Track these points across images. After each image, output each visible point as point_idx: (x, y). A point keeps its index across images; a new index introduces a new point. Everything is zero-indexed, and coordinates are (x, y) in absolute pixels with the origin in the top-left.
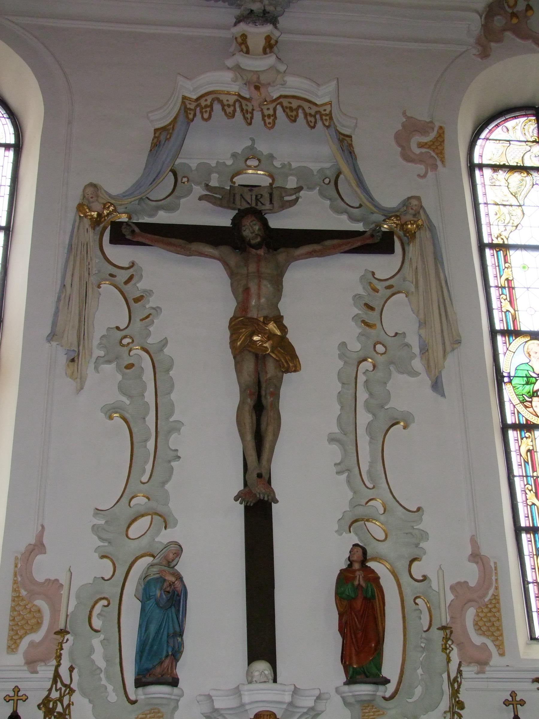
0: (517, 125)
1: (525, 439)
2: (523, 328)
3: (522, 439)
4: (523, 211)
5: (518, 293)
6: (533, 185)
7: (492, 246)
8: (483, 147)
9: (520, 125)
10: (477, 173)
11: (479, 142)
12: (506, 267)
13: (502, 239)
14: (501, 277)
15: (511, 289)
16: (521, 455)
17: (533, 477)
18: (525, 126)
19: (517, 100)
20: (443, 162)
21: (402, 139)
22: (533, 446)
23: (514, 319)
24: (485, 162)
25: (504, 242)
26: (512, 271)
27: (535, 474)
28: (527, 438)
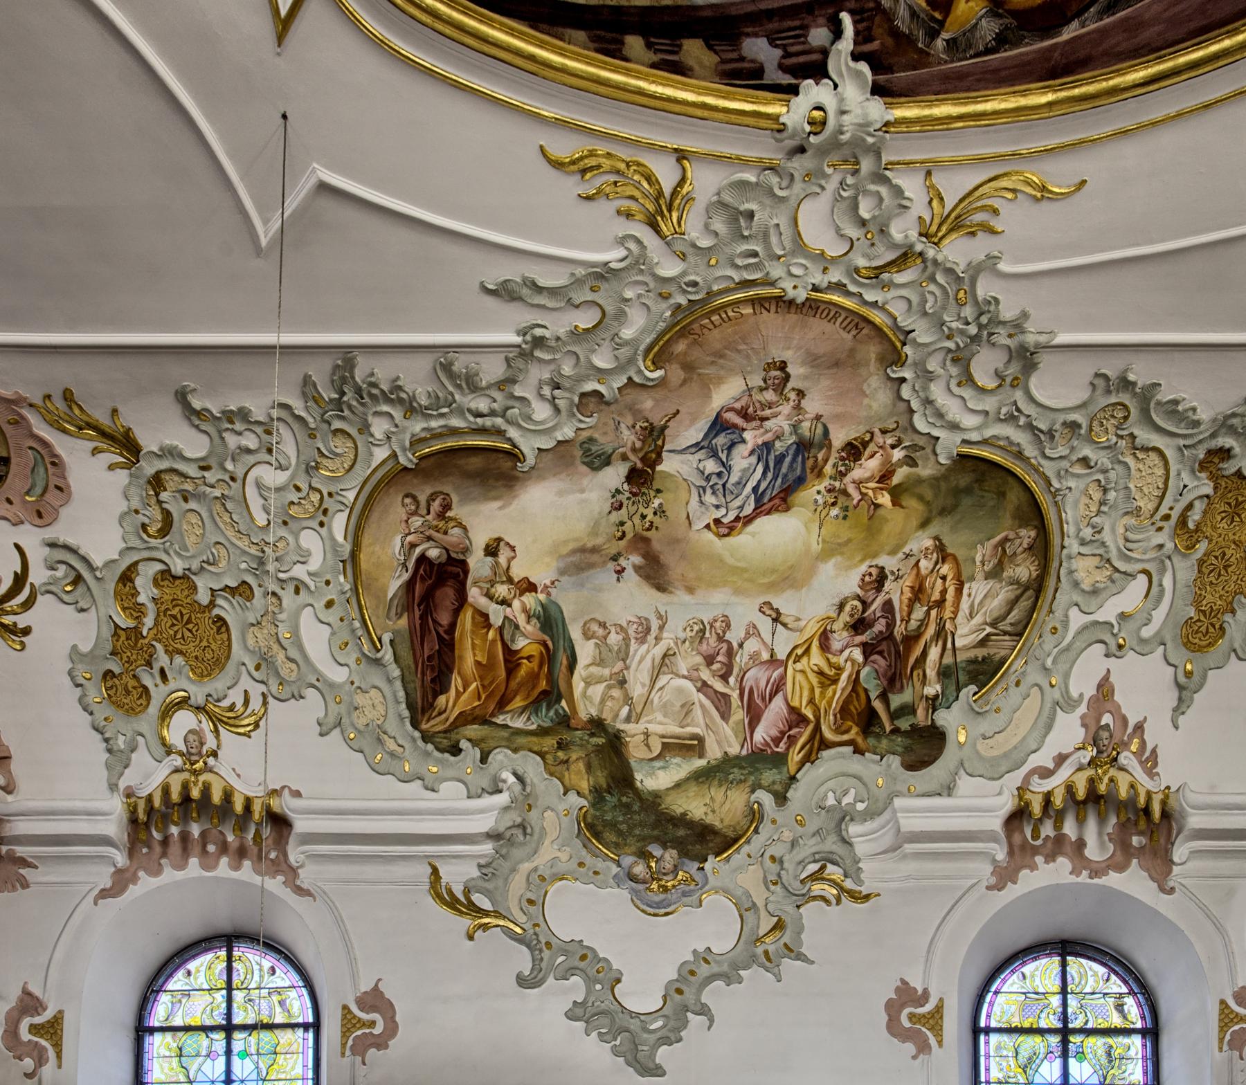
8: (991, 1004)
10: (982, 1038)
11: (989, 997)
24: (993, 1024)
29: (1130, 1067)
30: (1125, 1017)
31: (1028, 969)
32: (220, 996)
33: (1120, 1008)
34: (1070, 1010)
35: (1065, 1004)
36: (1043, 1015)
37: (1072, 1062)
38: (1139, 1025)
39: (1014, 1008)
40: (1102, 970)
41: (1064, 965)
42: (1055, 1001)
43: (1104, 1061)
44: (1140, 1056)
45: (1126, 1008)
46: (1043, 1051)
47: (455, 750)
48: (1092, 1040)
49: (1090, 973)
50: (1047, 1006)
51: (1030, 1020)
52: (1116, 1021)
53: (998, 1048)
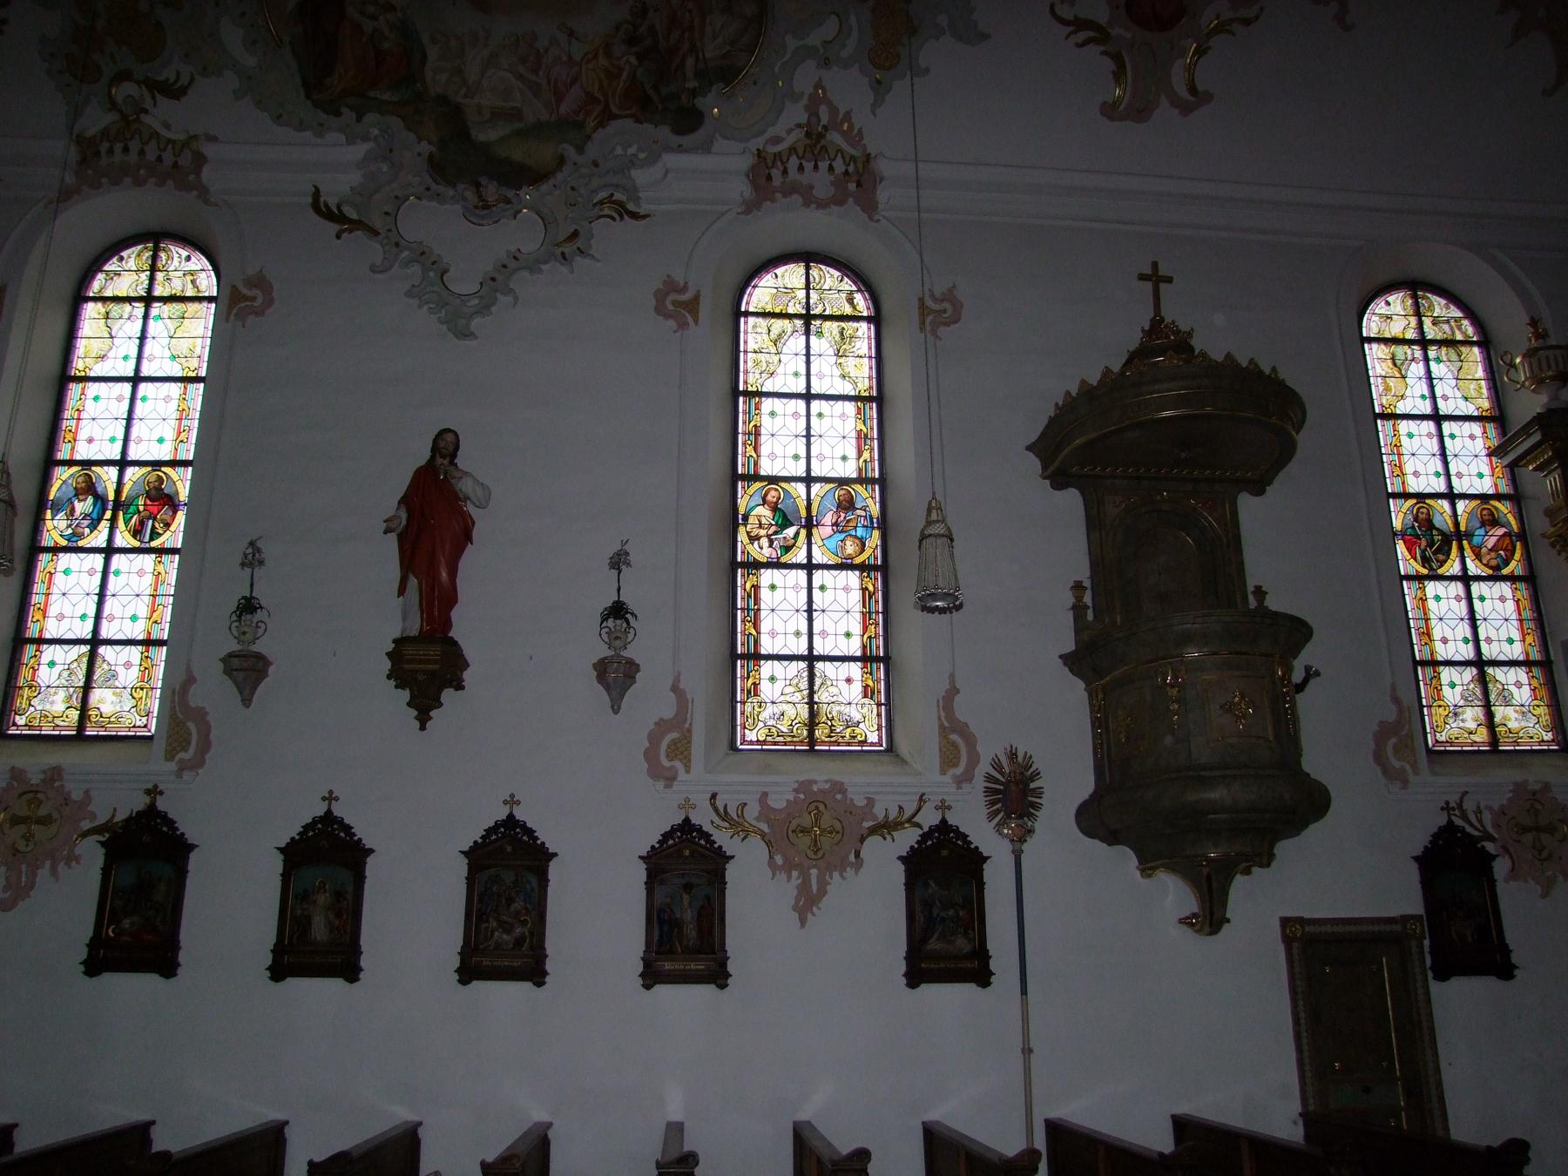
2: (762, 473)
5: (763, 439)
7: (746, 394)
8: (750, 295)
15: (757, 434)
19: (791, 247)
20: (696, 322)
21: (660, 297)
23: (756, 464)
29: (858, 344)
30: (854, 308)
31: (779, 271)
32: (144, 277)
33: (850, 301)
37: (812, 338)
39: (768, 298)
40: (837, 274)
41: (808, 269)
42: (801, 294)
43: (838, 338)
46: (790, 330)
47: (338, 114)
48: (828, 324)
52: (848, 310)
53: (755, 327)
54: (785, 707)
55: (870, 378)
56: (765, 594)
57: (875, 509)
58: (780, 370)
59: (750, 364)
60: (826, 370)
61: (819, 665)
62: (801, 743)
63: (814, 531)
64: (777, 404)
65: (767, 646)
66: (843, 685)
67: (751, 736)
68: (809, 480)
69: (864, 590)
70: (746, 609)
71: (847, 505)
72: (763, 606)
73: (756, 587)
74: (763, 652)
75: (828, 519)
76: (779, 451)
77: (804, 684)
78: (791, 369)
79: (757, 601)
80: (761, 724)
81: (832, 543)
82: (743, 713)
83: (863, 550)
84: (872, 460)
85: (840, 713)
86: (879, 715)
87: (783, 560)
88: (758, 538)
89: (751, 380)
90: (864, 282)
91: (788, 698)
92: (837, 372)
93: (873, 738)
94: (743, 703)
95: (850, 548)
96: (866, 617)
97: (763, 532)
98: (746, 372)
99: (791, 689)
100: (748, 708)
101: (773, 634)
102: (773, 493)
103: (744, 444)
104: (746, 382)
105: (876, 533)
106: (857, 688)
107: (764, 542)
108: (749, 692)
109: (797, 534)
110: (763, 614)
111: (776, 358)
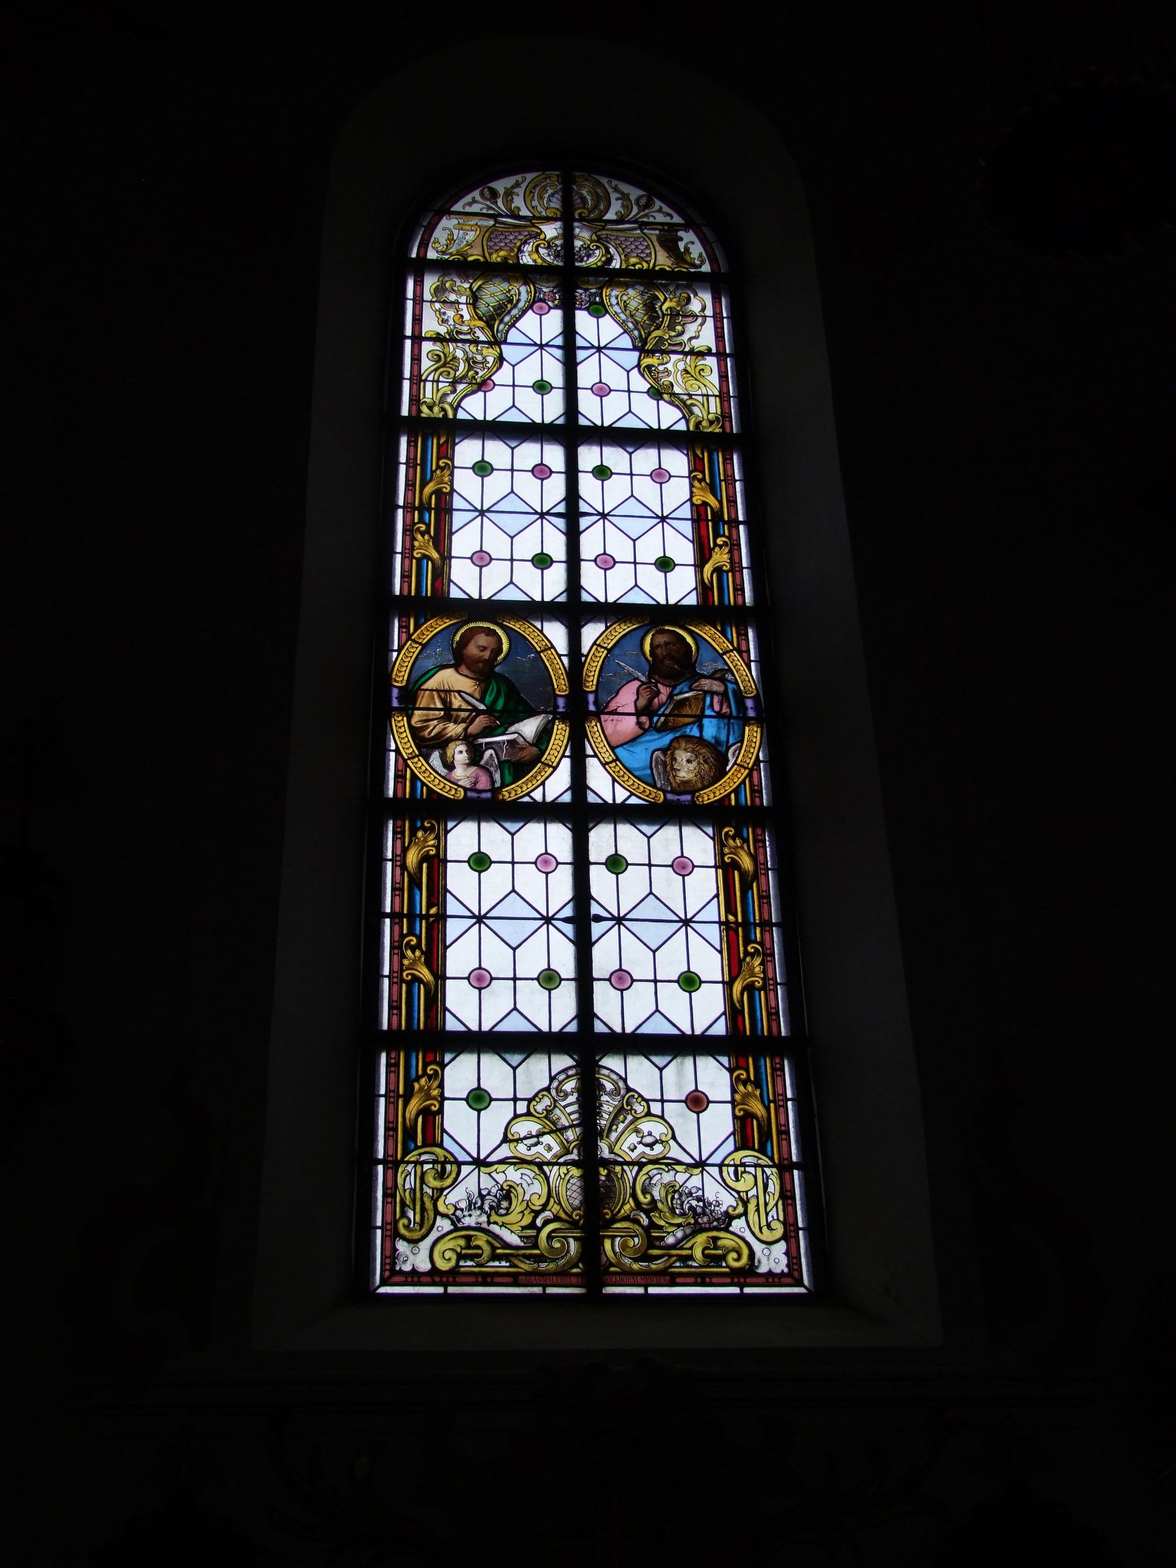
0: (517, 185)
1: (420, 834)
3: (413, 834)
4: (501, 354)
6: (534, 302)
9: (524, 186)
12: (438, 467)
13: (443, 409)
14: (424, 484)
16: (404, 867)
17: (427, 916)
18: (534, 188)
22: (437, 847)
24: (432, 255)
25: (446, 415)
26: (452, 474)
27: (433, 911)
28: (425, 830)
29: (691, 329)
31: (500, 186)
33: (669, 242)
34: (578, 244)
35: (568, 235)
36: (527, 248)
38: (706, 268)
43: (641, 316)
44: (709, 312)
45: (681, 245)
49: (614, 196)
50: (537, 236)
51: (502, 253)
52: (663, 260)
54: (513, 1174)
55: (723, 396)
56: (459, 879)
57: (747, 675)
58: (502, 376)
59: (426, 364)
60: (614, 377)
61: (612, 1062)
62: (562, 1277)
63: (593, 728)
64: (496, 451)
65: (463, 1008)
66: (677, 1114)
67: (417, 1259)
68: (574, 610)
69: (726, 867)
70: (404, 917)
71: (674, 666)
72: (452, 907)
73: (437, 863)
74: (451, 1025)
75: (627, 698)
76: (497, 545)
77: (568, 1112)
78: (528, 373)
79: (438, 892)
80: (444, 1225)
81: (638, 757)
82: (389, 1194)
83: (720, 772)
84: (736, 567)
85: (671, 1188)
86: (786, 1196)
87: (508, 794)
88: (441, 742)
89: (429, 392)
90: (702, 213)
91: (522, 1149)
92: (640, 384)
93: (774, 1259)
94: (392, 1164)
95: (686, 768)
96: (736, 936)
97: (454, 729)
98: (417, 380)
99: (533, 1127)
100: (407, 1179)
101: (480, 979)
102: (482, 640)
103: (409, 530)
104: (415, 400)
105: (753, 734)
106: (719, 1123)
107: (459, 753)
108: (410, 1134)
109: (544, 735)
110: (453, 928)
111: (491, 355)
